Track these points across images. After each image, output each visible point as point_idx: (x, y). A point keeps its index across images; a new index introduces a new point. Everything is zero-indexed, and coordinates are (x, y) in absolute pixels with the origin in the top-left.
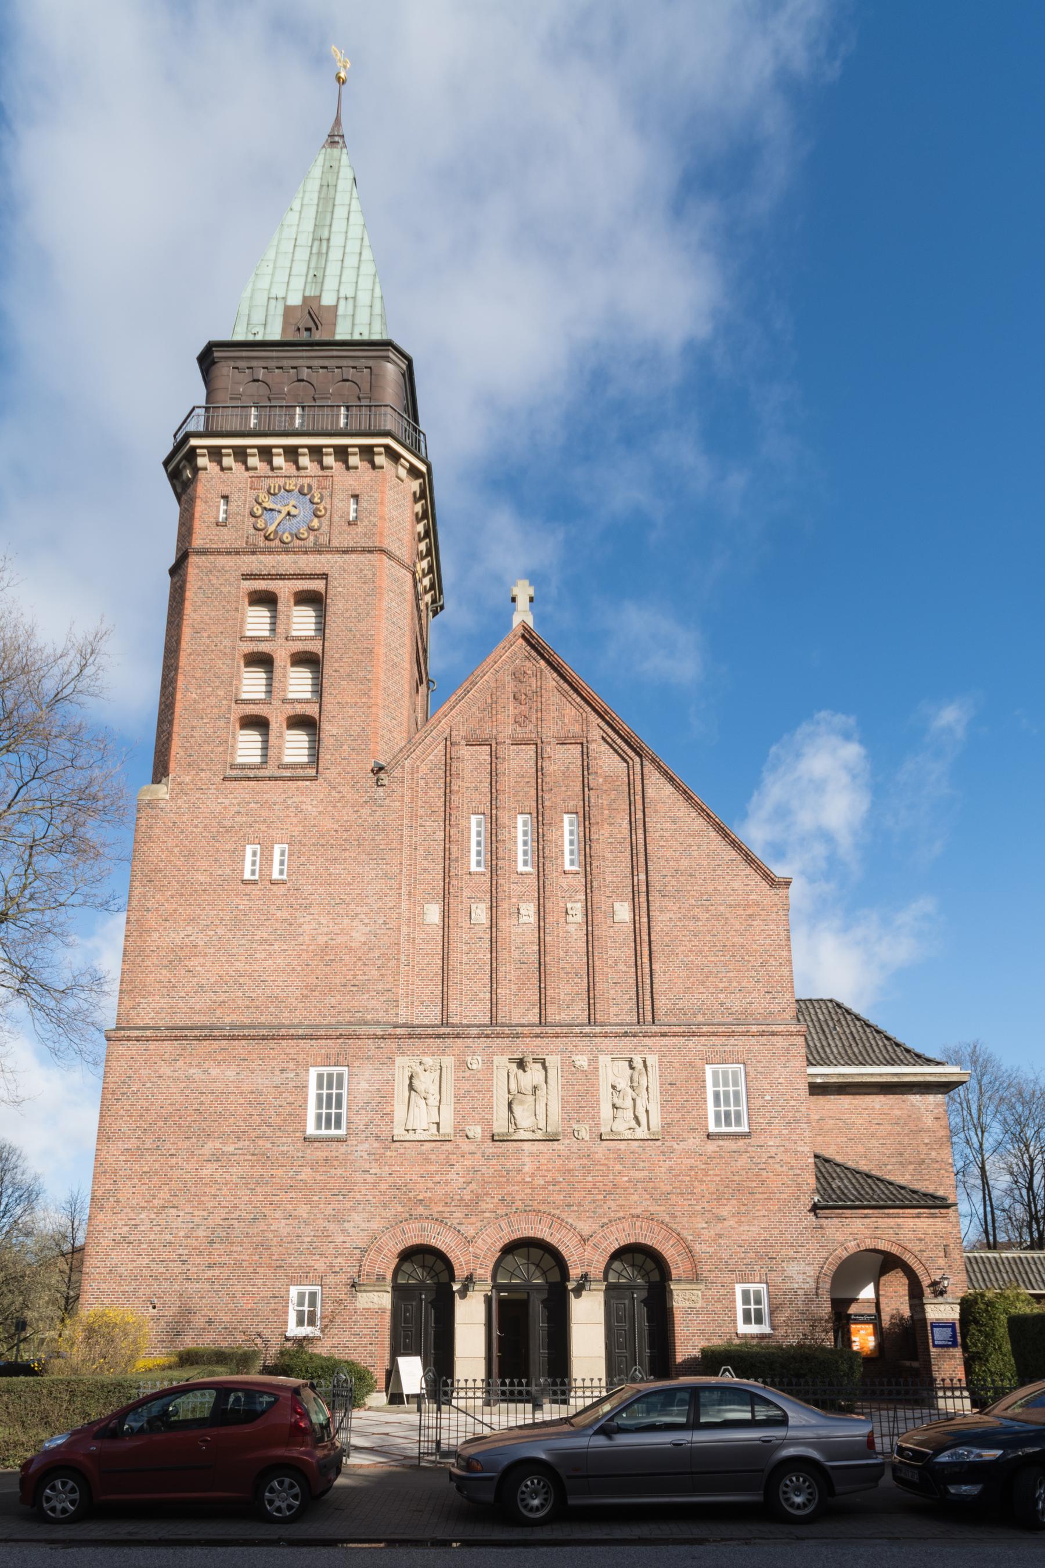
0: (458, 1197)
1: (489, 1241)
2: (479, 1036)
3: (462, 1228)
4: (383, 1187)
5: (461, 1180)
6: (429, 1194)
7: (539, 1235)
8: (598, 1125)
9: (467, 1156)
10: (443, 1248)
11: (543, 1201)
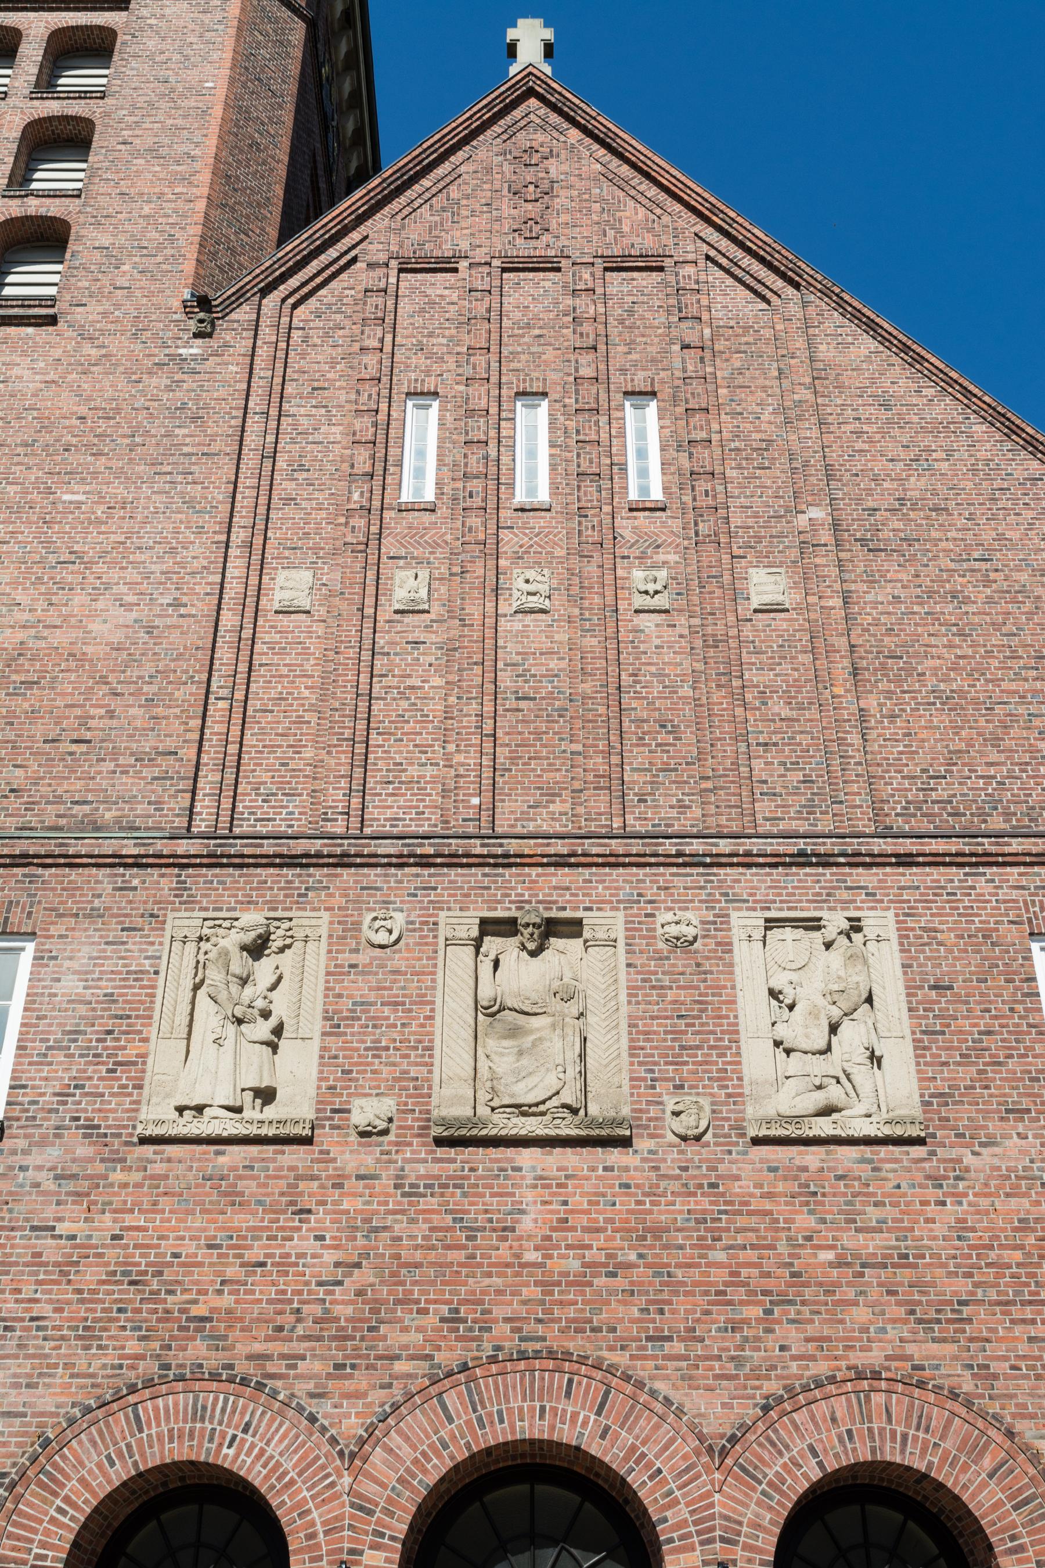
0: (317, 1310)
1: (405, 1451)
2: (400, 862)
3: (324, 1409)
4: (90, 1275)
5: (330, 1257)
6: (227, 1300)
7: (566, 1434)
8: (736, 1098)
9: (350, 1184)
10: (257, 1476)
11: (578, 1325)
